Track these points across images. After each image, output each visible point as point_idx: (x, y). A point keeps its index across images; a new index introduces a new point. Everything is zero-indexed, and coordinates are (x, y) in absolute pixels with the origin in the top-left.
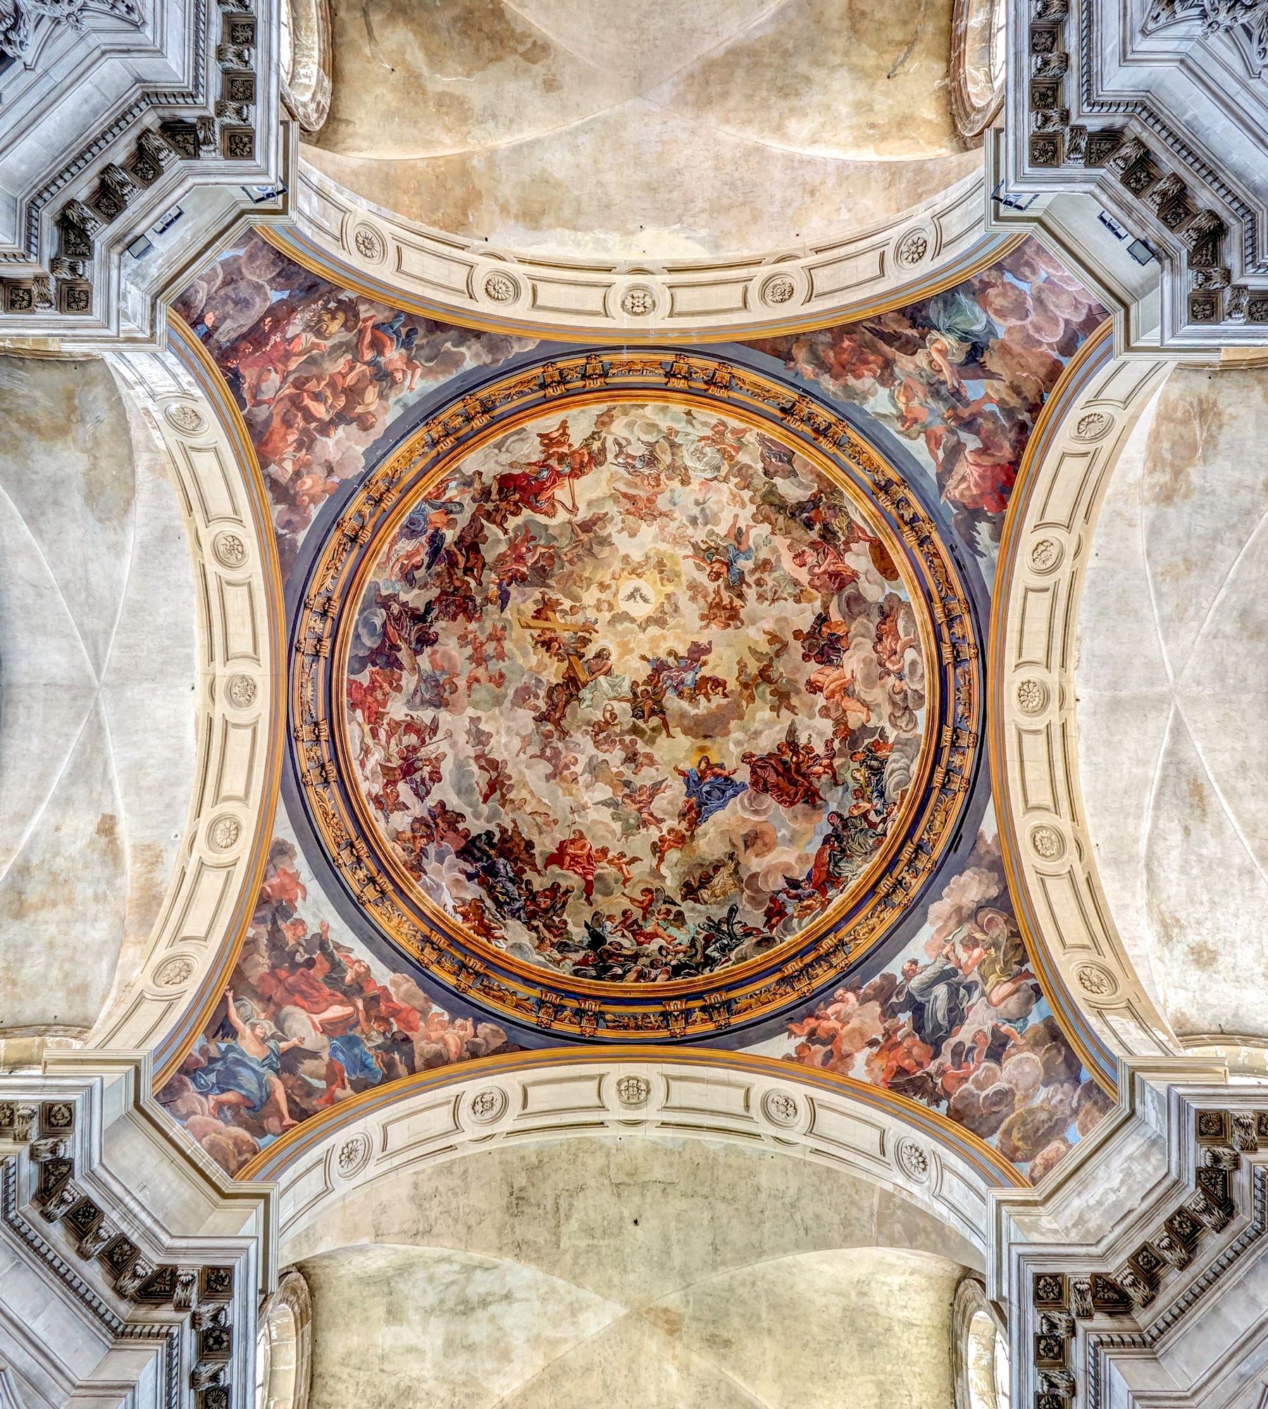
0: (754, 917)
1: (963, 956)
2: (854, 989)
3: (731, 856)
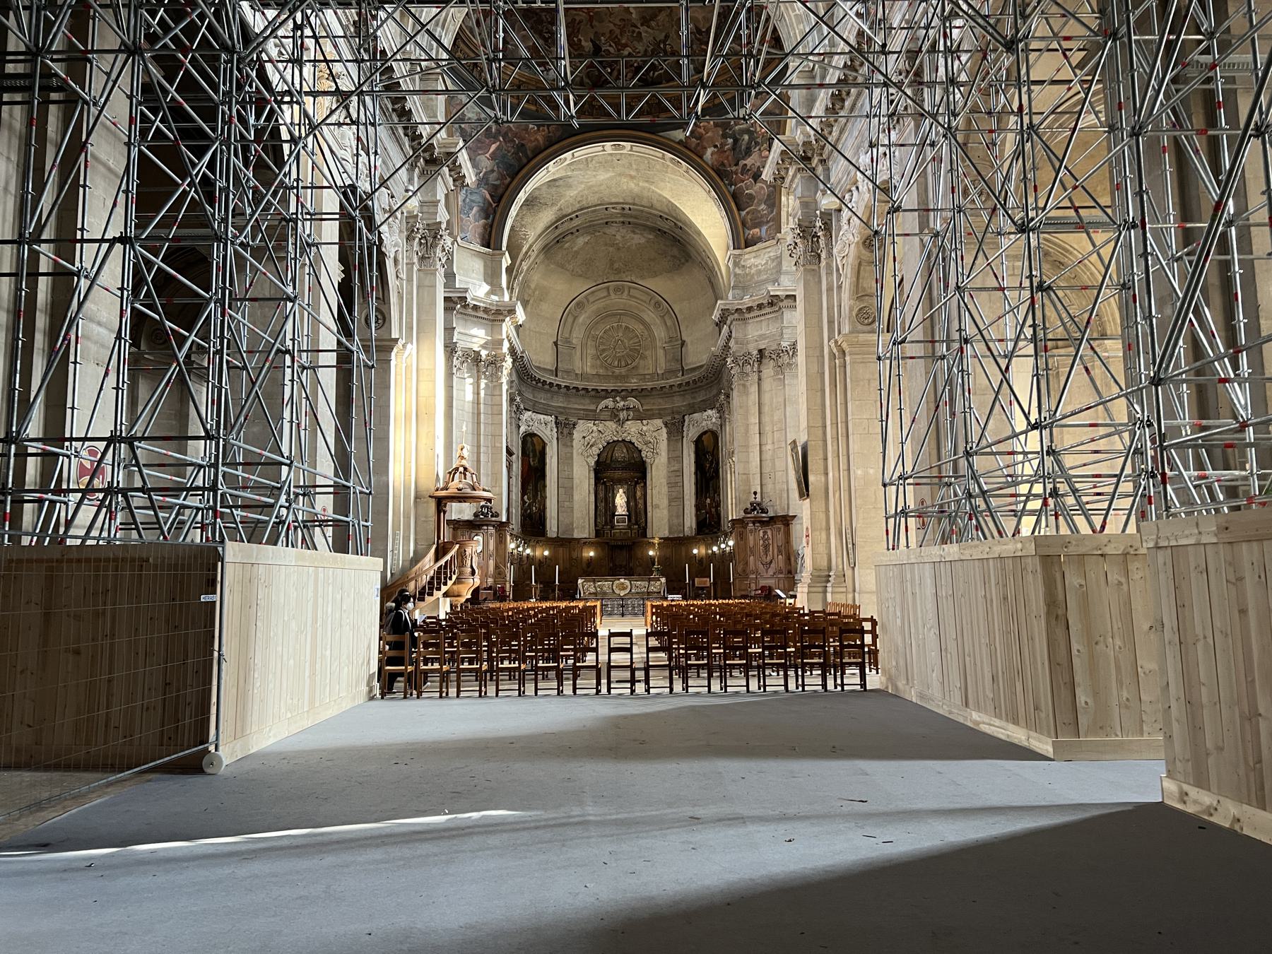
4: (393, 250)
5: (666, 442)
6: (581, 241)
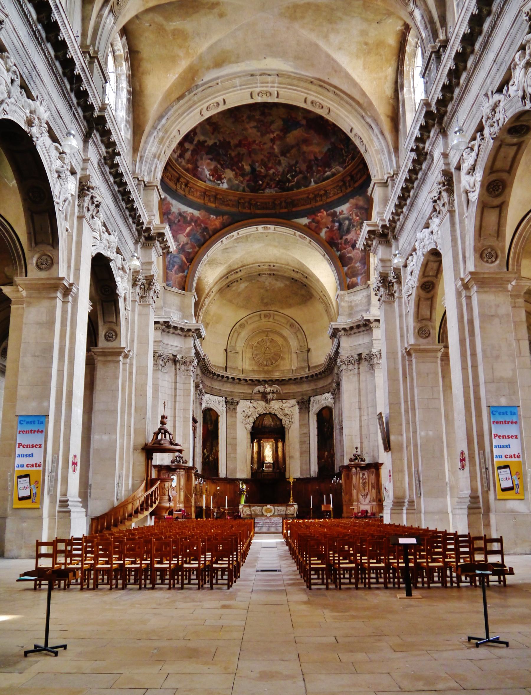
0: (304, 167)
1: (354, 217)
2: (326, 211)
3: (298, 145)
4: (124, 292)
5: (298, 414)
6: (243, 285)
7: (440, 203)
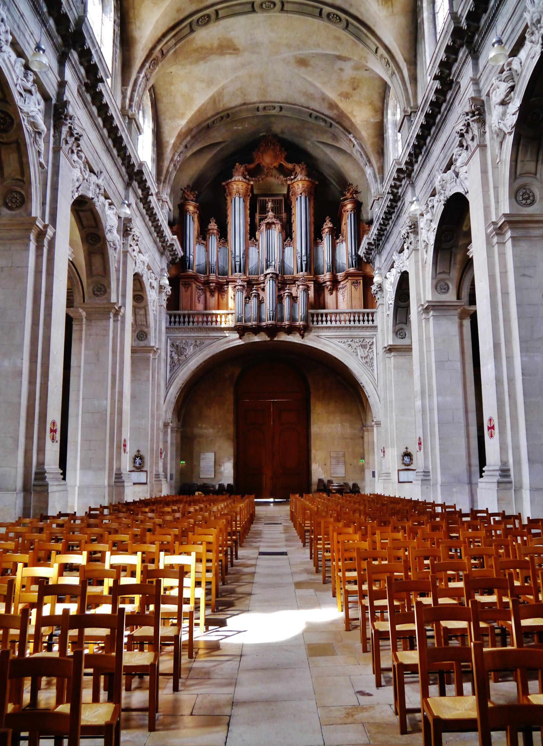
7: (468, 137)
